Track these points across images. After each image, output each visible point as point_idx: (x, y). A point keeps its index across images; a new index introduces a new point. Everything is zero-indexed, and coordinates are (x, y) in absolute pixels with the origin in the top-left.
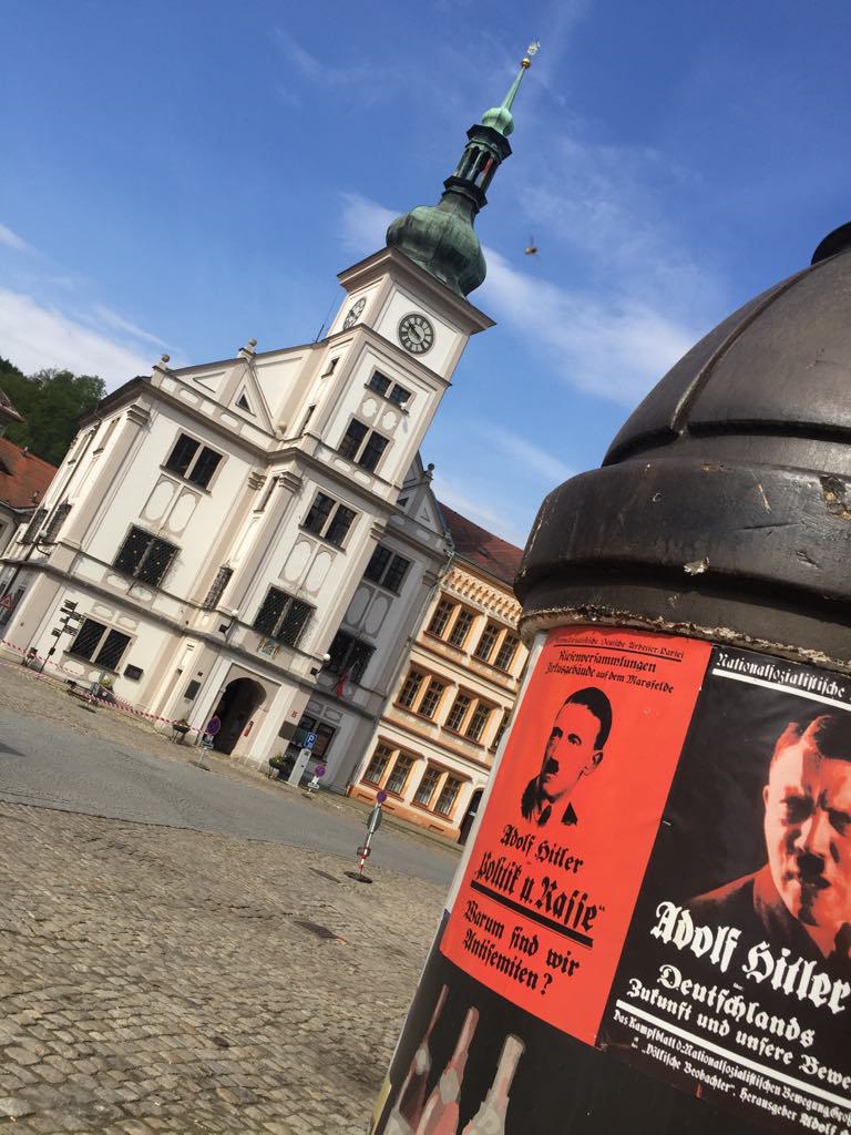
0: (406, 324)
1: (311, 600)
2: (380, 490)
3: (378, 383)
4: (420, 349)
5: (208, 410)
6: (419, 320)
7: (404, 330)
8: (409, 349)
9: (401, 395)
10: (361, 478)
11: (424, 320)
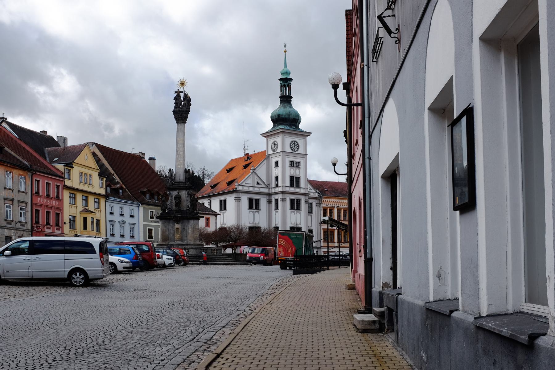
1: (300, 226)
2: (302, 191)
3: (292, 164)
5: (251, 189)
9: (298, 163)
10: (297, 190)
11: (295, 141)
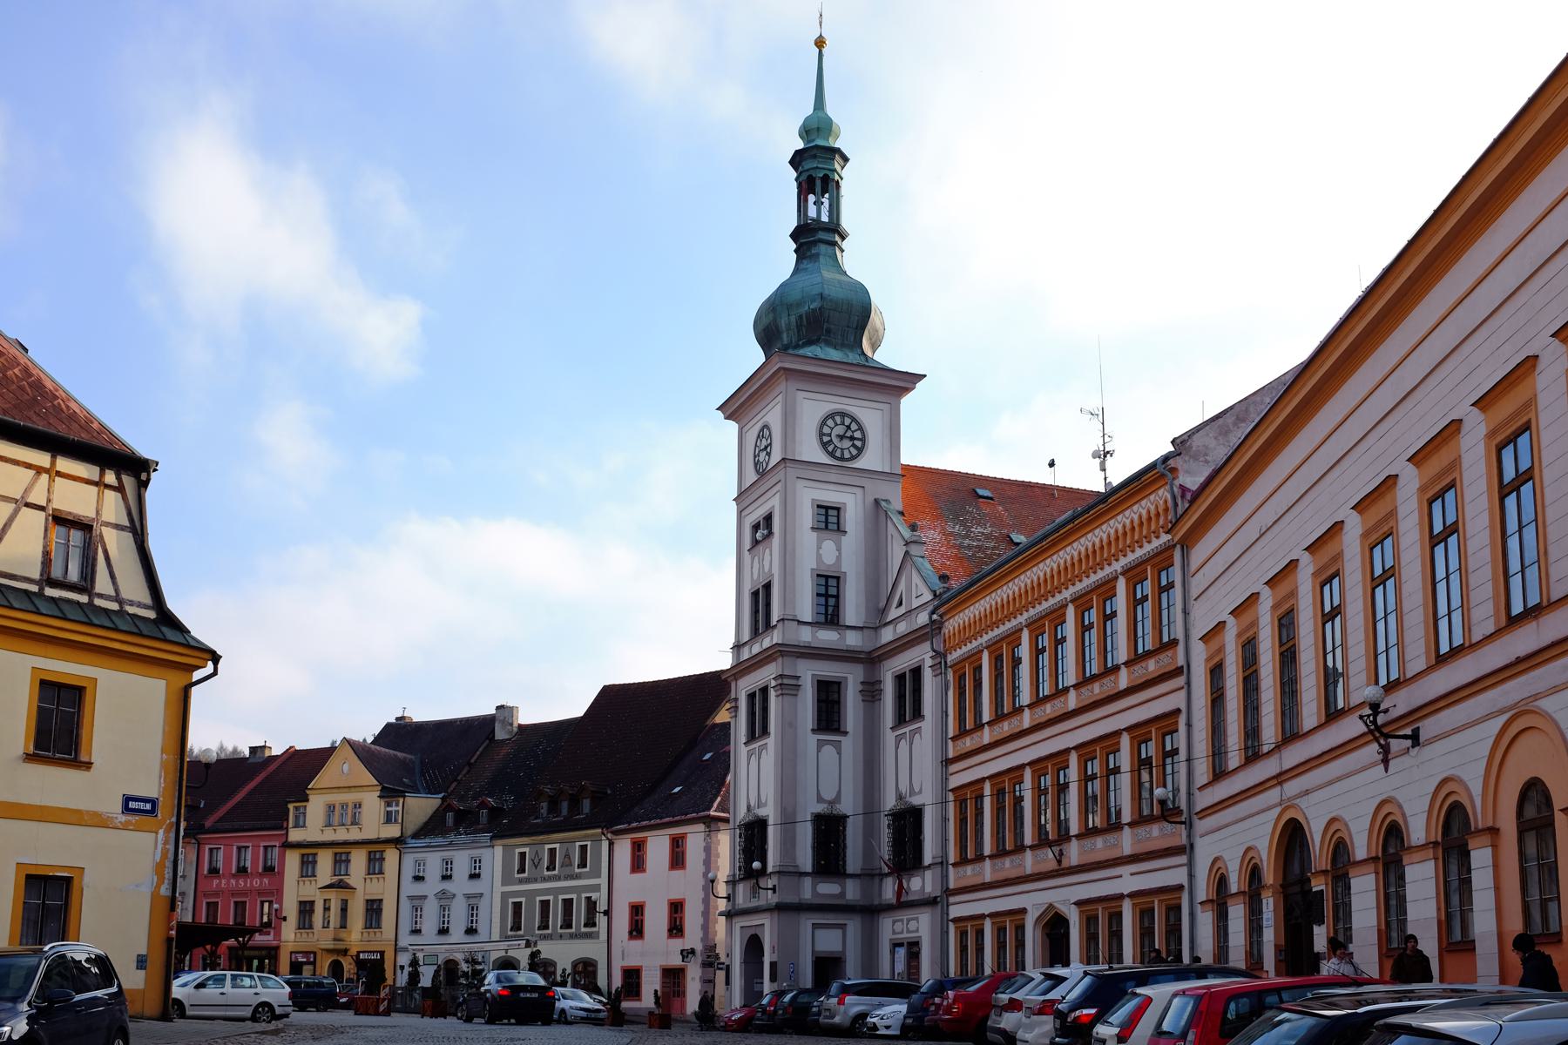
0: (826, 430)
4: (854, 452)
6: (838, 419)
7: (826, 439)
8: (842, 459)
